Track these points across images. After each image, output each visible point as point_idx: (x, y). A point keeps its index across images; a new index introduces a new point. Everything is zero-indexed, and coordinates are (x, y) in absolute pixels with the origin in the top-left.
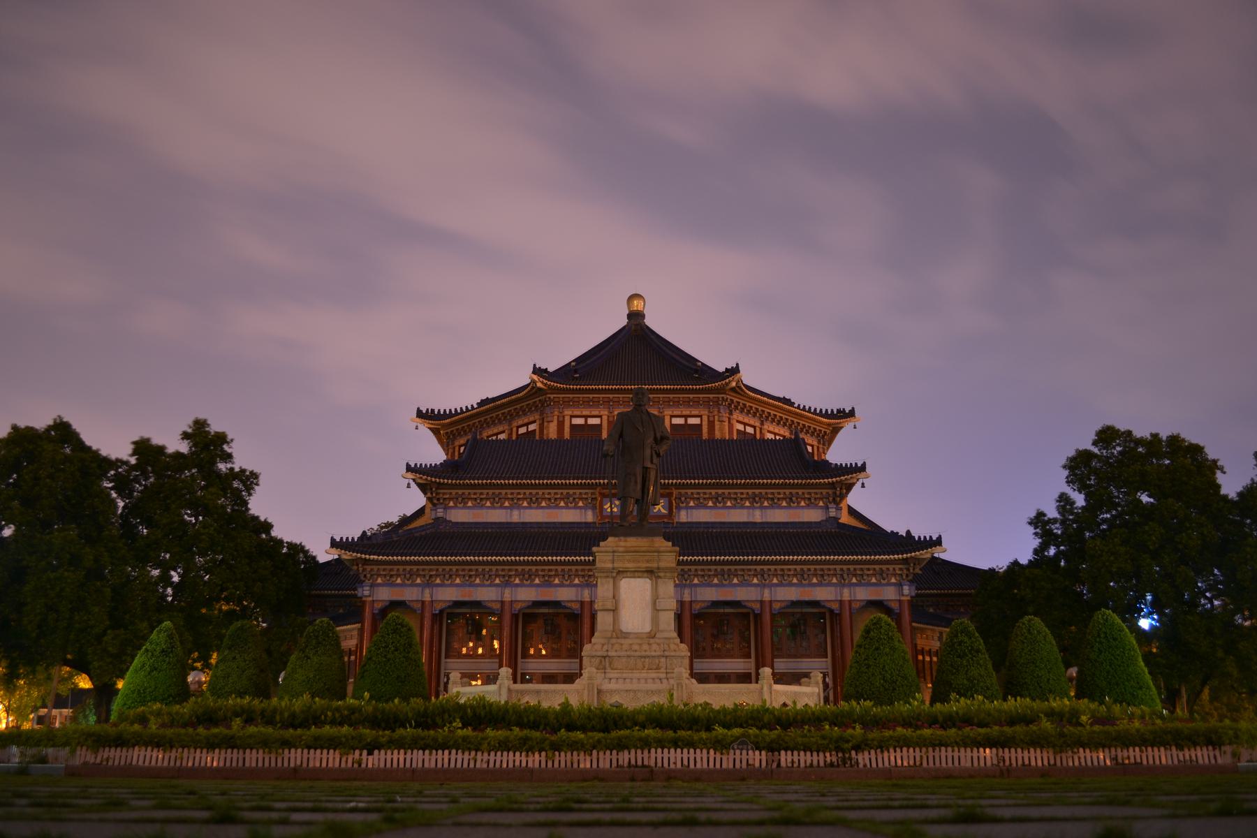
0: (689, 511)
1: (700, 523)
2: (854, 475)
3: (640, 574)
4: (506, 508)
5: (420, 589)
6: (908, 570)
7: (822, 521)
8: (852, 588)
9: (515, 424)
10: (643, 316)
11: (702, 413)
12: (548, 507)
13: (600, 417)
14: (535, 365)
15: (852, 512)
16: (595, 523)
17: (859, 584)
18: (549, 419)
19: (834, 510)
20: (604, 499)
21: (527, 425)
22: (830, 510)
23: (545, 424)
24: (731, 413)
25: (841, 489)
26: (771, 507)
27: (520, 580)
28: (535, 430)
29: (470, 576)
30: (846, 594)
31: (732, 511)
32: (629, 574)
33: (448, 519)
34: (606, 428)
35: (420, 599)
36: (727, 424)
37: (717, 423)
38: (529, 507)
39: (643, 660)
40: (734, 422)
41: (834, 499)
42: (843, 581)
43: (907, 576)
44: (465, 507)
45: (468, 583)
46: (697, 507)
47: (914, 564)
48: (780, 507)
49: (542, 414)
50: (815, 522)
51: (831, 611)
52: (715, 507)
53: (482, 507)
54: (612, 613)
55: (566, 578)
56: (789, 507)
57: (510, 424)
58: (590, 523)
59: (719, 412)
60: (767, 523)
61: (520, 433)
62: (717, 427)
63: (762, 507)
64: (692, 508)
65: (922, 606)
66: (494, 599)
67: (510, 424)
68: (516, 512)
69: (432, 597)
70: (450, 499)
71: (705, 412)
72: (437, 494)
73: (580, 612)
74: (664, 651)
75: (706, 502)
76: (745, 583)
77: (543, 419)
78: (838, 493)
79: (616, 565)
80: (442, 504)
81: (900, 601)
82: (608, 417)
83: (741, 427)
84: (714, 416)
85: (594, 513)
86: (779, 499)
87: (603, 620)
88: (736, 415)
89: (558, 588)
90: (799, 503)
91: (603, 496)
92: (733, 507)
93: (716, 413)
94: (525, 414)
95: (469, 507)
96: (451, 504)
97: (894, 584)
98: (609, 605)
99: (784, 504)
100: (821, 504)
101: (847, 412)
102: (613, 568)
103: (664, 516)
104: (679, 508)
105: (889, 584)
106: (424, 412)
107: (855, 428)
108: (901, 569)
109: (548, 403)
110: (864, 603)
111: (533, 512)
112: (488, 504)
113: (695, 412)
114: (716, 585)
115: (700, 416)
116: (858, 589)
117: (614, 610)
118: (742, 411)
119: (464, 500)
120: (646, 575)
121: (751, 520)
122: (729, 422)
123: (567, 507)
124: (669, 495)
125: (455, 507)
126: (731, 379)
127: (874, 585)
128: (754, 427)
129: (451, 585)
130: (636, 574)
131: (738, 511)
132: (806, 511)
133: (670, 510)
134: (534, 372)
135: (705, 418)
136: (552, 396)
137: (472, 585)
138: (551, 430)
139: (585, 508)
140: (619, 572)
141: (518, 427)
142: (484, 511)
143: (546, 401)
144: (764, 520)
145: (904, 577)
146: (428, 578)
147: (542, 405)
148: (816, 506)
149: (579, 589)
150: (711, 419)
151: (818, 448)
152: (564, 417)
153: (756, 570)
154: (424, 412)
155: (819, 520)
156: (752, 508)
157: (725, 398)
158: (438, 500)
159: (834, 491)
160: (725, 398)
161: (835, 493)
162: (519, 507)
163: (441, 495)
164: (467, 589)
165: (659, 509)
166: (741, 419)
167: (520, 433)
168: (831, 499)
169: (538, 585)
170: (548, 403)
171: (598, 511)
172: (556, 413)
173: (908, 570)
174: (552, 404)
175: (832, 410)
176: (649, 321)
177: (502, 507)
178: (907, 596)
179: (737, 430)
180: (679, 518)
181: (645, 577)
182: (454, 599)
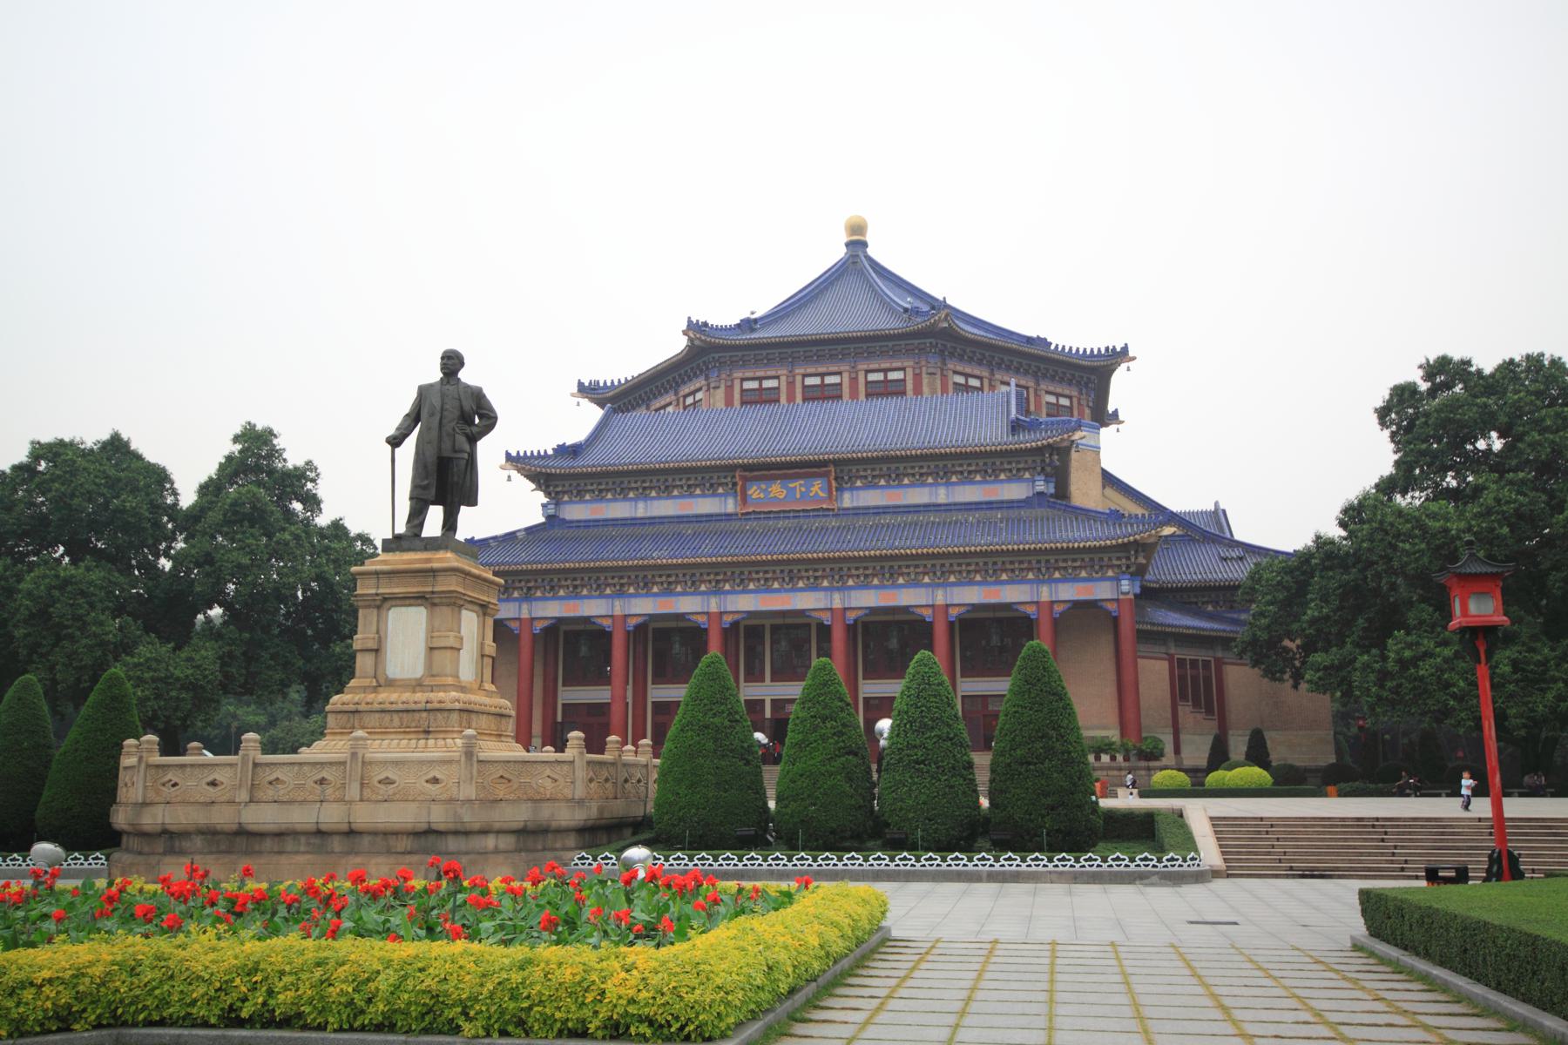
0: (855, 492)
1: (868, 508)
2: (1066, 436)
3: (412, 601)
4: (631, 499)
5: (517, 604)
6: (1128, 558)
7: (1027, 498)
8: (1053, 585)
9: (682, 393)
10: (864, 244)
11: (906, 364)
12: (681, 496)
13: (777, 377)
14: (689, 318)
15: (1109, 480)
16: (737, 514)
17: (1063, 580)
18: (717, 384)
19: (1042, 483)
20: (748, 484)
21: (693, 393)
22: (1037, 483)
25: (1051, 455)
27: (635, 589)
28: (701, 400)
29: (575, 587)
30: (1045, 593)
31: (910, 490)
32: (398, 602)
33: (561, 517)
35: (517, 616)
36: (938, 377)
37: (924, 376)
38: (658, 498)
39: (401, 714)
41: (1043, 469)
42: (1041, 577)
43: (1128, 567)
44: (582, 501)
45: (573, 595)
46: (866, 487)
47: (1136, 552)
48: (972, 482)
49: (707, 378)
50: (1019, 501)
52: (888, 486)
53: (602, 499)
54: (374, 654)
55: (689, 584)
56: (984, 482)
57: (676, 393)
60: (955, 504)
61: (687, 403)
62: (925, 380)
63: (948, 484)
65: (1196, 603)
66: (604, 613)
67: (676, 393)
68: (641, 505)
69: (530, 613)
70: (564, 493)
71: (909, 363)
72: (547, 487)
73: (706, 626)
74: (427, 702)
75: (876, 481)
76: (916, 584)
77: (708, 385)
78: (1047, 461)
79: (381, 591)
80: (554, 498)
81: (1117, 600)
82: (788, 377)
84: (920, 368)
85: (736, 501)
87: (363, 663)
88: (952, 365)
89: (680, 598)
90: (997, 476)
91: (745, 479)
93: (923, 363)
95: (587, 501)
96: (566, 498)
97: (1110, 579)
98: (372, 645)
99: (978, 478)
100: (1027, 475)
101: (1118, 349)
102: (377, 595)
103: (823, 500)
104: (840, 489)
105: (1104, 579)
106: (587, 384)
107: (1128, 369)
108: (1119, 559)
110: (1069, 605)
111: (662, 502)
112: (609, 496)
113: (898, 364)
114: (876, 587)
115: (903, 369)
116: (1061, 586)
117: (377, 651)
118: (961, 358)
119: (580, 493)
120: (419, 601)
121: (933, 500)
123: (703, 496)
124: (826, 475)
125: (571, 502)
127: (1084, 580)
128: (980, 378)
129: (555, 598)
130: (407, 602)
131: (917, 490)
132: (1006, 485)
133: (830, 492)
134: (688, 326)
135: (910, 372)
136: (716, 356)
137: (578, 596)
138: (718, 397)
139: (725, 495)
140: (385, 599)
141: (685, 397)
142: (603, 505)
144: (951, 500)
145: (1124, 569)
146: (525, 590)
147: (707, 368)
148: (1020, 479)
149: (706, 597)
150: (917, 371)
151: (1079, 400)
152: (732, 381)
153: (977, 564)
154: (587, 384)
155: (1024, 497)
157: (934, 343)
159: (1041, 458)
160: (934, 343)
161: (1043, 461)
162: (646, 498)
163: (551, 488)
164: (571, 602)
165: (817, 493)
167: (687, 403)
168: (1039, 469)
169: (656, 595)
171: (739, 498)
172: (724, 376)
173: (1128, 558)
175: (1099, 350)
176: (872, 251)
177: (625, 498)
178: (1128, 593)
179: (955, 384)
180: (842, 502)
181: (419, 605)
182: (557, 615)
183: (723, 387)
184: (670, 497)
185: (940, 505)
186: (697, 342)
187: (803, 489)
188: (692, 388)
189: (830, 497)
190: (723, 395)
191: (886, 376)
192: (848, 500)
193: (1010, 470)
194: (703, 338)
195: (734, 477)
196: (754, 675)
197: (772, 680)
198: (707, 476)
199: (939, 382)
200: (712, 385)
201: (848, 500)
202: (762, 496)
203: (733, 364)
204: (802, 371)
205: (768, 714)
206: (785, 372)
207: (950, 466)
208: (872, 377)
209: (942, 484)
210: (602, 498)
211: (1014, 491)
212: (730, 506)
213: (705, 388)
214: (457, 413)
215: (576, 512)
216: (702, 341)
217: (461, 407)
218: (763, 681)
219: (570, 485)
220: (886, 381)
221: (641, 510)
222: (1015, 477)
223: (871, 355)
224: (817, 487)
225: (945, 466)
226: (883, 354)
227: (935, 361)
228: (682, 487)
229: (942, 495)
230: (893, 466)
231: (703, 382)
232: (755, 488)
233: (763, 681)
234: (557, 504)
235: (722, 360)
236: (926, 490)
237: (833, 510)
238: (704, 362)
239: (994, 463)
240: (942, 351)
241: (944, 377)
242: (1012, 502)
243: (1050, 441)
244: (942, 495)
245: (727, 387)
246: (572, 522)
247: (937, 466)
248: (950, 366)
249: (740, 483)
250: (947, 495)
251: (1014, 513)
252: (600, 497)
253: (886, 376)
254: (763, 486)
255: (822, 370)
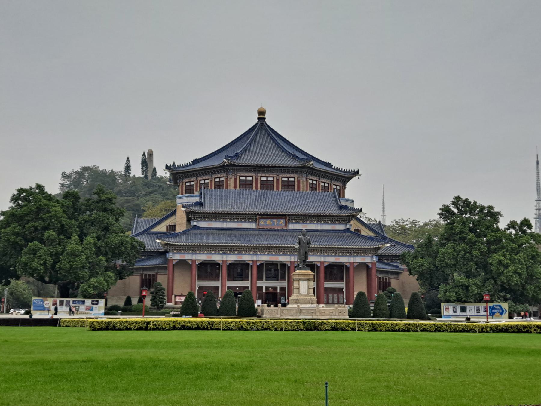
1: (297, 229)
11: (295, 176)
12: (238, 222)
16: (256, 229)
24: (307, 176)
26: (325, 223)
33: (198, 226)
36: (305, 181)
37: (301, 180)
38: (230, 221)
40: (308, 180)
44: (205, 221)
46: (296, 223)
48: (328, 223)
50: (342, 230)
51: (346, 266)
52: (303, 223)
53: (212, 221)
58: (254, 229)
59: (302, 176)
60: (323, 230)
62: (301, 182)
63: (321, 224)
64: (294, 223)
68: (225, 224)
71: (296, 176)
72: (194, 216)
78: (351, 219)
80: (195, 220)
83: (311, 181)
84: (300, 178)
86: (328, 221)
90: (335, 222)
91: (260, 218)
92: (310, 223)
93: (301, 176)
96: (199, 220)
100: (344, 223)
104: (289, 223)
122: (306, 180)
123: (245, 222)
124: (285, 219)
125: (201, 220)
126: (308, 163)
135: (296, 178)
139: (252, 222)
142: (212, 223)
150: (299, 179)
156: (317, 223)
158: (194, 218)
161: (349, 219)
162: (226, 221)
163: (195, 216)
166: (311, 178)
168: (348, 221)
177: (219, 221)
179: (310, 183)
184: (234, 222)
185: (318, 230)
187: (277, 222)
189: (286, 225)
191: (288, 179)
192: (291, 226)
193: (339, 221)
195: (256, 217)
196: (260, 278)
197: (266, 280)
198: (247, 216)
199: (305, 182)
201: (291, 226)
202: (264, 223)
205: (264, 291)
207: (322, 218)
209: (319, 224)
210: (212, 220)
211: (341, 227)
212: (254, 226)
215: (203, 224)
218: (263, 281)
219: (202, 216)
220: (288, 181)
221: (225, 225)
222: (340, 223)
223: (284, 172)
224: (282, 222)
225: (321, 218)
226: (289, 172)
227: (304, 176)
228: (238, 219)
229: (319, 227)
230: (305, 217)
232: (262, 221)
233: (263, 280)
234: (197, 222)
236: (314, 225)
237: (286, 229)
239: (335, 219)
240: (307, 173)
241: (307, 181)
242: (340, 230)
243: (353, 214)
244: (319, 227)
246: (201, 228)
247: (318, 218)
248: (309, 177)
249: (258, 219)
250: (320, 227)
251: (340, 234)
252: (210, 220)
253: (288, 179)
254: (265, 221)
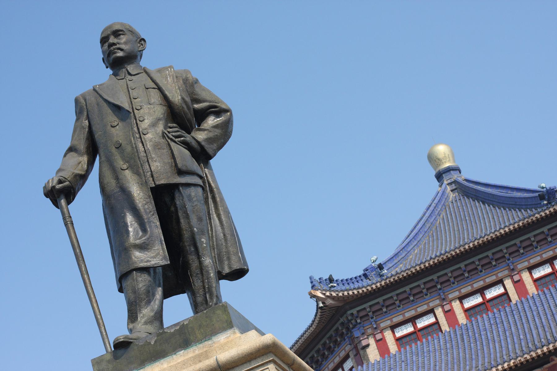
23: (361, 352)
34: (445, 322)
94: (331, 351)
109: (353, 322)
136: (354, 311)
143: (349, 321)
147: (348, 329)
170: (353, 322)
172: (369, 331)
174: (359, 321)
183: (372, 341)
186: (329, 302)
188: (337, 360)
190: (376, 352)
194: (334, 294)
200: (359, 347)
203: (378, 312)
204: (457, 294)
206: (438, 302)
208: (538, 273)
213: (352, 355)
214: (159, 111)
216: (331, 297)
217: (165, 97)
231: (348, 348)
235: (362, 314)
238: (342, 324)
245: (377, 341)
255: (478, 285)
